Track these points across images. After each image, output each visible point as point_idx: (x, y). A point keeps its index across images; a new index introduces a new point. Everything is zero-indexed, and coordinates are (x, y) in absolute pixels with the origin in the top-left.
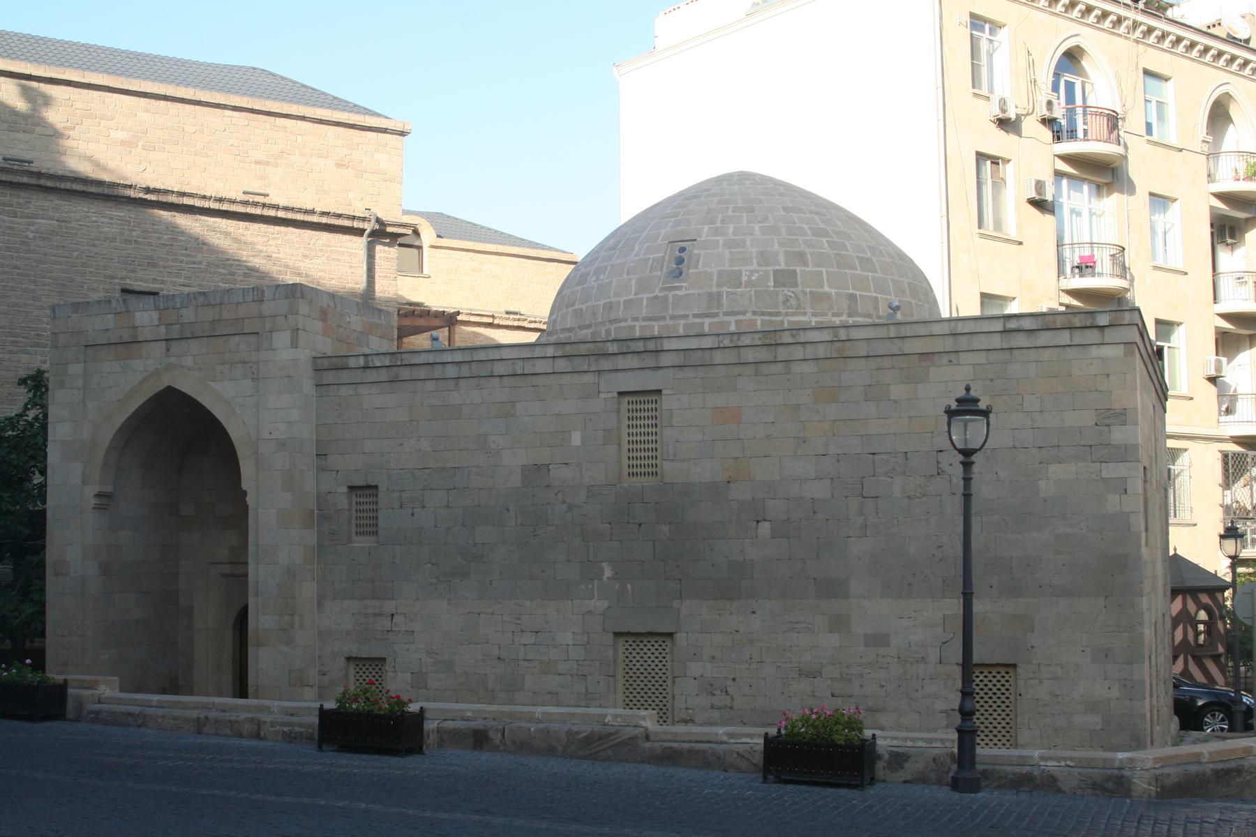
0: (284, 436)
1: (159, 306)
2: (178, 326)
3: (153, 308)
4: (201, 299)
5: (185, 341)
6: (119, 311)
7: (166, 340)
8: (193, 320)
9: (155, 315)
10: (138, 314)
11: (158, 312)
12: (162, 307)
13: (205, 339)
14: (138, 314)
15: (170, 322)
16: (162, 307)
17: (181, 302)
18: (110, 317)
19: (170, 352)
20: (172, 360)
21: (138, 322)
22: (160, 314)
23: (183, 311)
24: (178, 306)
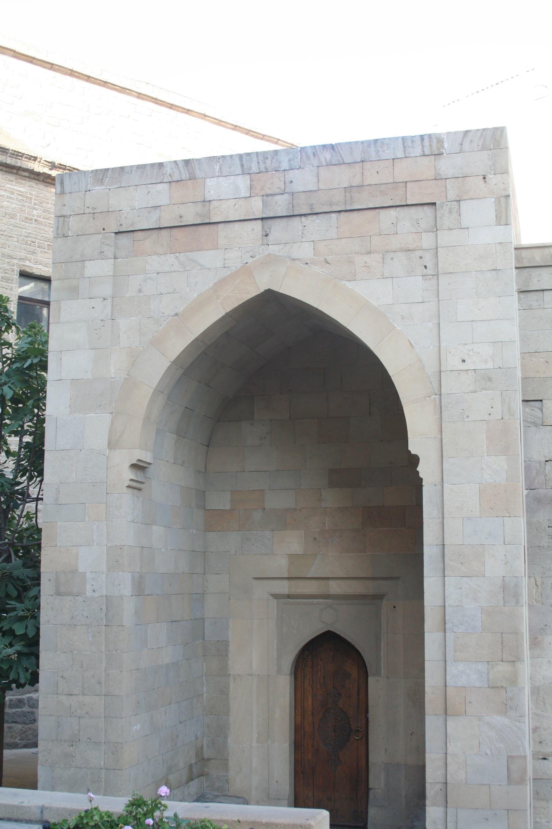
0: (490, 365)
1: (250, 168)
2: (286, 196)
3: (239, 170)
4: (328, 155)
5: (297, 219)
6: (176, 177)
7: (262, 219)
8: (312, 187)
9: (243, 183)
10: (210, 182)
11: (248, 177)
12: (254, 169)
13: (333, 215)
14: (210, 182)
15: (270, 192)
16: (254, 169)
17: (289, 160)
18: (160, 186)
19: (270, 237)
20: (273, 249)
21: (210, 194)
22: (251, 181)
23: (291, 175)
24: (285, 165)
